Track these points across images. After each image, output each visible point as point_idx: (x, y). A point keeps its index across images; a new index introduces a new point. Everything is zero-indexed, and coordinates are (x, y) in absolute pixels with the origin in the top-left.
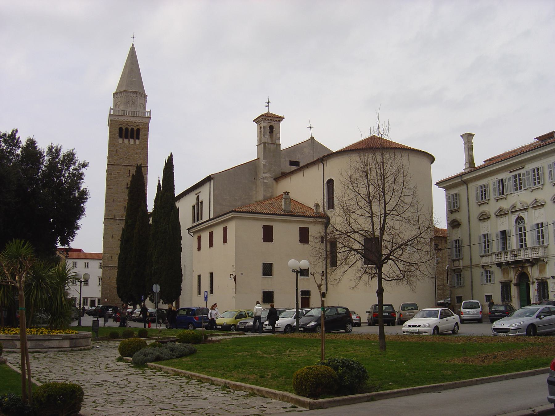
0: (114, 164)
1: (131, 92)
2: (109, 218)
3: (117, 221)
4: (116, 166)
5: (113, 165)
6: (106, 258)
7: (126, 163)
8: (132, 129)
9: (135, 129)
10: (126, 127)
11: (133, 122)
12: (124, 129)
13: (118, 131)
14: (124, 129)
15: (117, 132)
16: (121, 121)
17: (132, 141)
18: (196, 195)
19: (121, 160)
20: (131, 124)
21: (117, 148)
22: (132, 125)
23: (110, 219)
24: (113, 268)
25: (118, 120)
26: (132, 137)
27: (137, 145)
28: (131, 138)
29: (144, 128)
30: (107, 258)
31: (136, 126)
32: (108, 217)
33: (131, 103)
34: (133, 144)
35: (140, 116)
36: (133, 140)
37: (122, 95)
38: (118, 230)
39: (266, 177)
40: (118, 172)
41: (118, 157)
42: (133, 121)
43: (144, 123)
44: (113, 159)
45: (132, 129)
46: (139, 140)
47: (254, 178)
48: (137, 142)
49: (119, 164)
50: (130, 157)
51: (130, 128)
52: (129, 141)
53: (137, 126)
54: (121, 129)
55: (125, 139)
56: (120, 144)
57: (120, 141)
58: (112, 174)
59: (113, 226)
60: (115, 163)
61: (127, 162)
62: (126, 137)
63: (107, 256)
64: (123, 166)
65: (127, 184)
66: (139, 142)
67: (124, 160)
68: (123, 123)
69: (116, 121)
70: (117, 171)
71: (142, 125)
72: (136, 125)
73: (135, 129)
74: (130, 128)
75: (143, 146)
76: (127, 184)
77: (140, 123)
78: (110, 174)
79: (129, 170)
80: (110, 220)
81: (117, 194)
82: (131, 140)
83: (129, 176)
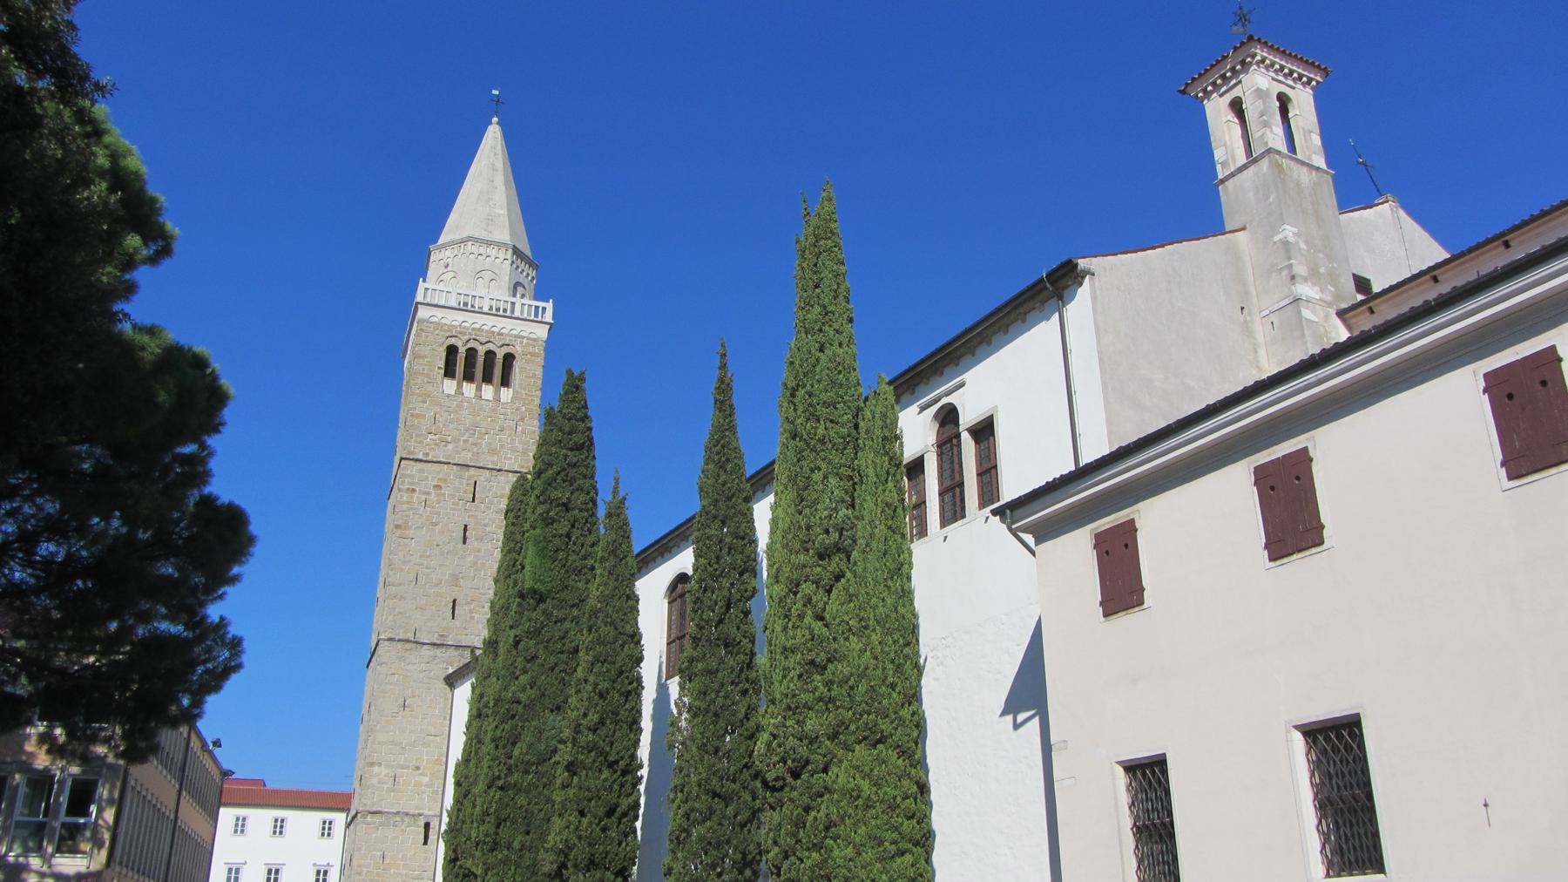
0: (425, 459)
1: (489, 243)
2: (397, 638)
3: (426, 652)
4: (430, 465)
5: (421, 461)
6: (375, 780)
7: (466, 457)
8: (490, 355)
9: (500, 354)
10: (469, 346)
11: (493, 332)
12: (462, 350)
13: (444, 355)
14: (462, 350)
15: (440, 359)
16: (455, 327)
17: (488, 391)
18: (923, 409)
19: (450, 446)
20: (488, 339)
21: (437, 409)
22: (489, 342)
23: (399, 640)
24: (398, 819)
25: (444, 321)
26: (488, 378)
27: (503, 404)
28: (483, 381)
29: (529, 353)
30: (379, 783)
31: (502, 346)
32: (393, 636)
33: (488, 276)
34: (491, 399)
35: (517, 314)
36: (491, 387)
37: (462, 250)
38: (427, 681)
39: (1306, 296)
40: (436, 486)
41: (439, 439)
42: (493, 329)
43: (528, 339)
44: (421, 442)
45: (490, 355)
46: (511, 390)
47: (1242, 308)
48: (506, 394)
49: (442, 460)
50: (480, 441)
51: (482, 350)
52: (479, 389)
53: (508, 345)
54: (452, 351)
55: (464, 384)
56: (449, 396)
57: (450, 386)
58: (414, 491)
59: (408, 667)
60: (427, 455)
61: (470, 454)
62: (469, 377)
63: (381, 773)
64: (455, 467)
65: (466, 526)
66: (511, 395)
67: (457, 447)
68: (461, 333)
69: (439, 326)
70: (433, 483)
71: (522, 343)
72: (501, 343)
73: (500, 354)
74: (482, 350)
75: (524, 409)
76: (466, 526)
77: (516, 336)
78: (408, 489)
79: (476, 482)
80: (400, 645)
81: (429, 556)
82: (483, 386)
83: (473, 501)
